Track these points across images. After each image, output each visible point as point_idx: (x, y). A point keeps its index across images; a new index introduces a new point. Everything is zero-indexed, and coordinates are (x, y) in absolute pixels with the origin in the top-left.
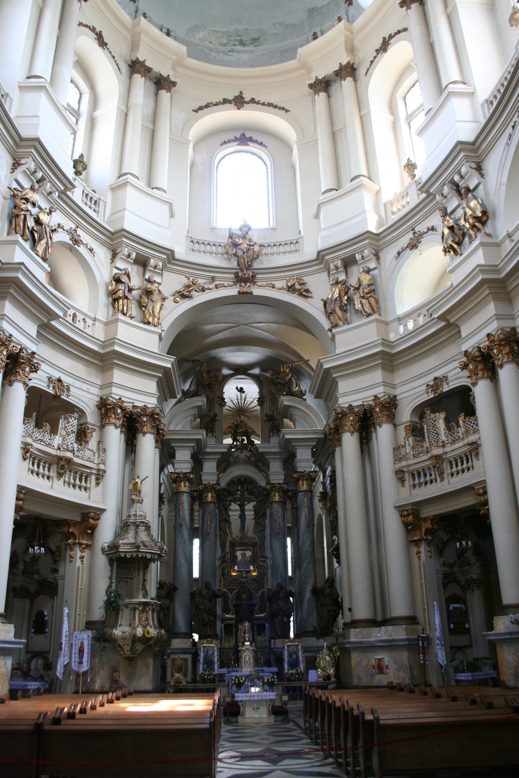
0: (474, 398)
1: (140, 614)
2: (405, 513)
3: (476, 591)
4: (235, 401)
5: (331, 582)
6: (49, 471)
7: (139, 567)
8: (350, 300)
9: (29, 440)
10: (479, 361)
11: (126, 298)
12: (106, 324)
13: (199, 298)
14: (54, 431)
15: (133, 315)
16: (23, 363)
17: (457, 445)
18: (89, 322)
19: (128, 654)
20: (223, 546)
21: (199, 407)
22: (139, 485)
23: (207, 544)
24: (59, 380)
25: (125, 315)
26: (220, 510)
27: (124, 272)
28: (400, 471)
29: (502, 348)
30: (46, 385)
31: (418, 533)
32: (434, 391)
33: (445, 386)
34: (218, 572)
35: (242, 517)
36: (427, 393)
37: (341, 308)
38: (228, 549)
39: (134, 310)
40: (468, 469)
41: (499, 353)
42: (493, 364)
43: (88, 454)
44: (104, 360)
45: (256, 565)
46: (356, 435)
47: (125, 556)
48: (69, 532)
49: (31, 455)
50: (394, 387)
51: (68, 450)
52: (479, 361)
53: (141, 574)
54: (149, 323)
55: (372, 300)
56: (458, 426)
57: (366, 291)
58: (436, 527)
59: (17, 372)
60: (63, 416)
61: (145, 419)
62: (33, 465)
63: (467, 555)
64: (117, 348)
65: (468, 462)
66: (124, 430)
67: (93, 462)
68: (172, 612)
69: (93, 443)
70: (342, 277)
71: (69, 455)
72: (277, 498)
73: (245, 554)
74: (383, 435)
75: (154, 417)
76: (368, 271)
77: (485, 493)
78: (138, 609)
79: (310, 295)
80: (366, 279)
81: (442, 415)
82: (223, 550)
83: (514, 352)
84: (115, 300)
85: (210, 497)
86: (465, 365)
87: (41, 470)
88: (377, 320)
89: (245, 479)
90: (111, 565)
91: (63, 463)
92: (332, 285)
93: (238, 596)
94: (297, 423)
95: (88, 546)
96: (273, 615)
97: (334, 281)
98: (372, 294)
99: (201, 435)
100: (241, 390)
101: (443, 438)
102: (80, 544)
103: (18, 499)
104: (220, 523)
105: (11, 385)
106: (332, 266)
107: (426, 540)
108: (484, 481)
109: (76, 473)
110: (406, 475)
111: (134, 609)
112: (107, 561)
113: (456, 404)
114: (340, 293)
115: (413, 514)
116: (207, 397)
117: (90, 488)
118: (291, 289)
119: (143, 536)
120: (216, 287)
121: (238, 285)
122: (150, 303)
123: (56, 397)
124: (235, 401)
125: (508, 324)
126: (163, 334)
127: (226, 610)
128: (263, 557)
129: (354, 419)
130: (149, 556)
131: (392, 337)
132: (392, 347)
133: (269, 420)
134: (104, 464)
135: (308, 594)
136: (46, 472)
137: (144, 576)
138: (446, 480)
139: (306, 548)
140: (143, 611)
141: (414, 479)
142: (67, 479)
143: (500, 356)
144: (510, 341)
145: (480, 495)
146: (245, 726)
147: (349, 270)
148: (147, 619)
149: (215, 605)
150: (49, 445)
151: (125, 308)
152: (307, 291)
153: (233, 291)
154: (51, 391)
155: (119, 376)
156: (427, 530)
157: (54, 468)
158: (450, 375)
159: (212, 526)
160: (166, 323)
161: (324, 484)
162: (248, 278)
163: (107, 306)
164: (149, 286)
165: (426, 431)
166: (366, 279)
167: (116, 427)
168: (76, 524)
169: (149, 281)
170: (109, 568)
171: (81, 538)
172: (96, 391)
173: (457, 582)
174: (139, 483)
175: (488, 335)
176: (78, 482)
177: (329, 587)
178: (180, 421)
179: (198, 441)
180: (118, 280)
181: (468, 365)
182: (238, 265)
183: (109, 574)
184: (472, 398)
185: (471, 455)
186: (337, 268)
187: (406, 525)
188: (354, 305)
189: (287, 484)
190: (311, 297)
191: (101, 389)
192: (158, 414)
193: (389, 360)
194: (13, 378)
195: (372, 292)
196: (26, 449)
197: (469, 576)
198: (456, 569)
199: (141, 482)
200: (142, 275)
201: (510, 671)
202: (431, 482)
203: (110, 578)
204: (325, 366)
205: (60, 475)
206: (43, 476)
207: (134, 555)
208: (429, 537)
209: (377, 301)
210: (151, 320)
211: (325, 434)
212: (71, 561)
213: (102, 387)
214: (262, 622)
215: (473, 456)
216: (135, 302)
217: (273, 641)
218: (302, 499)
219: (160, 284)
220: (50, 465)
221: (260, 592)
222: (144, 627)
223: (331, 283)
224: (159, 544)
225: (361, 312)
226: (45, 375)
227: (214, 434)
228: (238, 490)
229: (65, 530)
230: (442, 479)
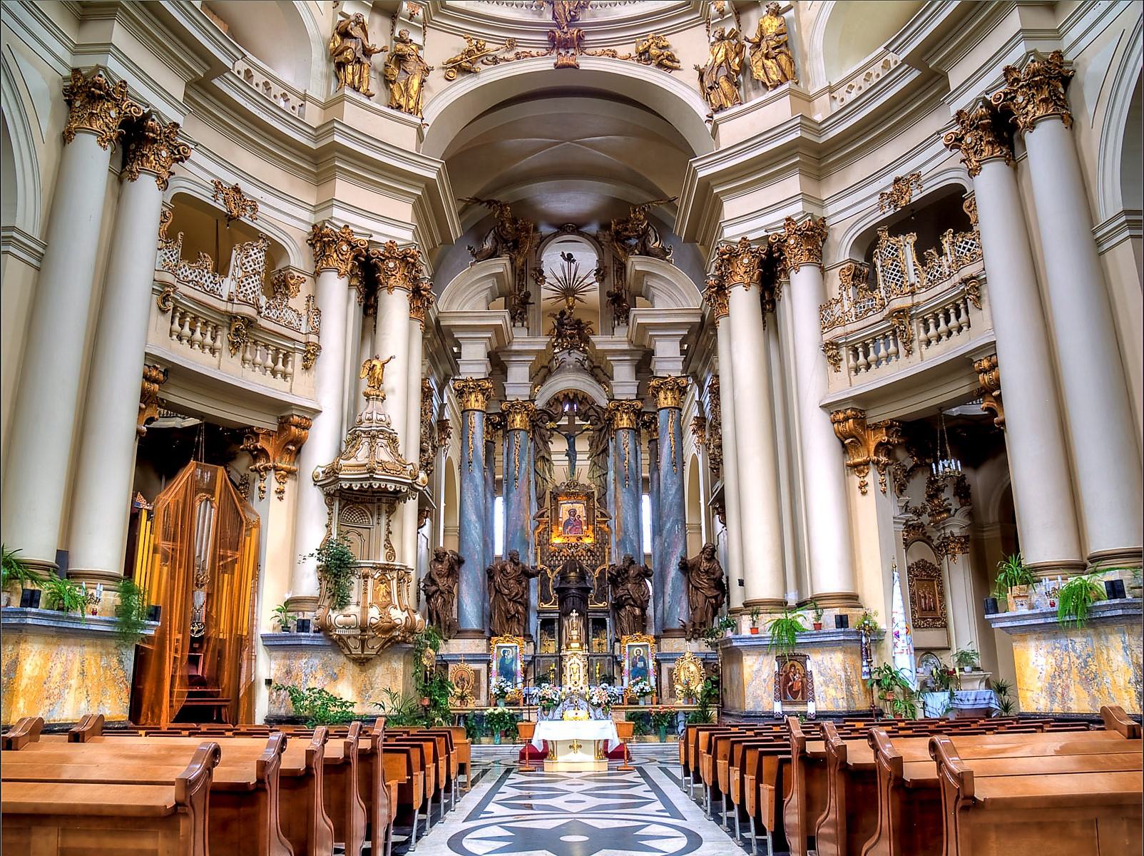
0: (973, 205)
2: (841, 416)
3: (959, 556)
4: (560, 274)
5: (711, 552)
6: (214, 339)
7: (379, 509)
8: (744, 67)
9: (169, 278)
10: (984, 128)
11: (359, 61)
12: (325, 107)
13: (489, 75)
14: (221, 268)
15: (371, 91)
16: (155, 141)
17: (938, 289)
18: (295, 101)
20: (540, 499)
21: (498, 276)
22: (378, 369)
23: (514, 497)
24: (236, 189)
25: (357, 90)
26: (536, 443)
27: (353, 18)
28: (832, 344)
29: (1033, 91)
30: (210, 195)
31: (863, 451)
32: (895, 203)
33: (914, 193)
34: (533, 540)
35: (571, 454)
36: (881, 208)
37: (728, 78)
38: (547, 503)
39: (374, 85)
40: (960, 329)
41: (1029, 101)
42: (1015, 127)
43: (290, 316)
44: (321, 161)
45: (591, 527)
46: (754, 290)
47: (350, 488)
48: (256, 448)
49: (175, 309)
50: (821, 204)
51: (246, 303)
52: (984, 128)
53: (383, 521)
54: (399, 107)
55: (783, 59)
56: (941, 253)
57: (772, 43)
58: (895, 440)
59: (143, 155)
60: (238, 246)
61: (391, 265)
62: (182, 326)
63: (943, 496)
64: (337, 139)
65: (958, 316)
66: (355, 282)
67: (298, 331)
68: (455, 600)
69: (298, 302)
70: (729, 27)
71: (249, 311)
72: (625, 422)
73: (575, 511)
74: (801, 288)
75: (406, 260)
76: (777, 13)
77: (994, 366)
79: (676, 64)
80: (772, 25)
81: (911, 238)
82: (540, 506)
83: (1059, 99)
84: (340, 66)
85: (518, 421)
86: (956, 140)
87: (198, 335)
88: (790, 92)
89: (576, 395)
90: (330, 505)
91: (237, 324)
92: (712, 44)
93: (563, 576)
94: (656, 301)
95: (291, 473)
96: (618, 606)
97: (717, 35)
98: (783, 49)
99: (500, 317)
100: (569, 258)
101: (913, 279)
102: (276, 469)
103: (146, 377)
104: (535, 463)
105: (133, 180)
106: (713, 10)
107: (877, 463)
108: (993, 344)
109: (266, 346)
110: (843, 352)
111: (366, 577)
112: (323, 498)
113: (938, 218)
114: (726, 54)
115: (855, 418)
116: (512, 261)
117: (292, 375)
118: (644, 56)
119: (384, 455)
120: (518, 56)
121: (555, 55)
122: (404, 75)
123: (230, 218)
124: (560, 274)
125: (1046, 48)
126: (426, 131)
127: (544, 598)
128: (603, 515)
129: (750, 263)
130: (391, 487)
131: (818, 118)
132: (819, 133)
133: (613, 302)
134: (317, 334)
135: (673, 570)
136: (208, 340)
137: (388, 525)
138: (916, 354)
141: (856, 357)
142: (248, 356)
143: (1030, 107)
144: (1050, 78)
145: (985, 371)
146: (555, 778)
147: (742, 18)
148: (389, 593)
149: (527, 588)
150: (211, 292)
151: (356, 78)
152: (671, 58)
153: (546, 64)
154: (220, 205)
155: (343, 189)
156: (880, 445)
157: (223, 335)
158: (924, 170)
159: (524, 467)
160: (431, 113)
161: (700, 404)
162: (572, 40)
163: (328, 77)
164: (400, 46)
165: (879, 269)
166: (772, 25)
167: (340, 275)
168: (268, 434)
169: (401, 40)
171: (277, 459)
172: (306, 215)
173: (927, 540)
174: (379, 366)
175: (1008, 71)
176: (270, 363)
177: (708, 560)
178: (469, 297)
179: (497, 329)
180: (345, 34)
181: (963, 138)
182: (554, 17)
184: (966, 203)
185: (966, 303)
186: (722, 13)
187: (841, 437)
188: (752, 73)
189: (642, 400)
190: (676, 69)
191: (315, 212)
192: (412, 256)
193: (817, 156)
194: (135, 167)
195: (783, 45)
196: (163, 294)
197: (948, 531)
198: (925, 519)
199: (383, 366)
200: (389, 32)
201: (1039, 684)
202: (888, 358)
204: (701, 174)
205: (235, 346)
206: (203, 347)
207: (366, 485)
208: (883, 459)
209: (791, 61)
210: (403, 102)
211: (703, 317)
212: (261, 498)
213: (316, 209)
214: (600, 615)
215: (970, 303)
216: (378, 76)
217: (617, 645)
218: (665, 422)
219: (420, 48)
220: (216, 328)
222: (384, 607)
223: (713, 40)
224: (410, 467)
225: (764, 84)
226: (209, 178)
228: (563, 414)
229: (248, 444)
230: (910, 352)
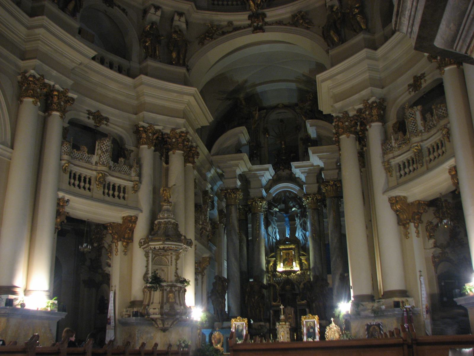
1: (167, 295)
19: (161, 326)
47: (155, 248)
78: (166, 290)
140: (171, 291)
170: (145, 259)
183: (145, 264)
203: (147, 266)
221: (302, 284)
227: (258, 158)
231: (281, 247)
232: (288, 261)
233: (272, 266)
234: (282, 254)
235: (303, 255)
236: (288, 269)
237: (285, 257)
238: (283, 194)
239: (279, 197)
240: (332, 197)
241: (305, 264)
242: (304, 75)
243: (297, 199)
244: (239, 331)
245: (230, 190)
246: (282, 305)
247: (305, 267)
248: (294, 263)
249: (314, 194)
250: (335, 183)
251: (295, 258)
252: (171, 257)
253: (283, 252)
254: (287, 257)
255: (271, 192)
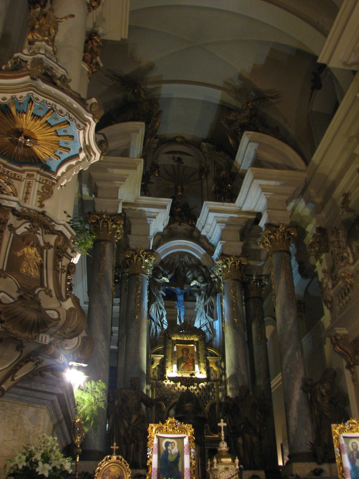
139: (289, 327)
231: (174, 338)
232: (185, 361)
233: (155, 369)
234: (175, 349)
235: (212, 355)
236: (188, 375)
237: (180, 355)
238: (178, 256)
239: (172, 261)
240: (281, 251)
241: (214, 371)
242: (241, 77)
243: (202, 269)
244: (171, 459)
245: (107, 215)
246: (222, 420)
247: (214, 375)
248: (197, 366)
249: (238, 257)
250: (288, 230)
251: (199, 359)
252: (29, 184)
253: (177, 347)
254: (185, 356)
255: (159, 252)
